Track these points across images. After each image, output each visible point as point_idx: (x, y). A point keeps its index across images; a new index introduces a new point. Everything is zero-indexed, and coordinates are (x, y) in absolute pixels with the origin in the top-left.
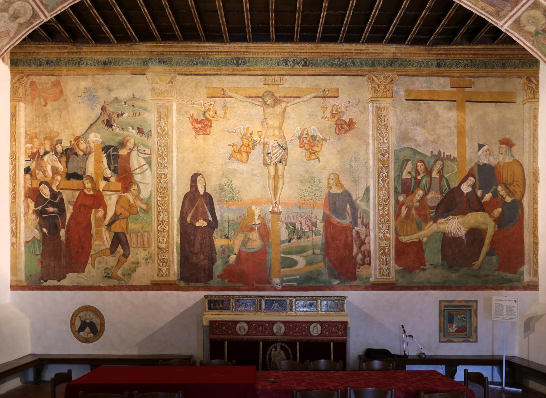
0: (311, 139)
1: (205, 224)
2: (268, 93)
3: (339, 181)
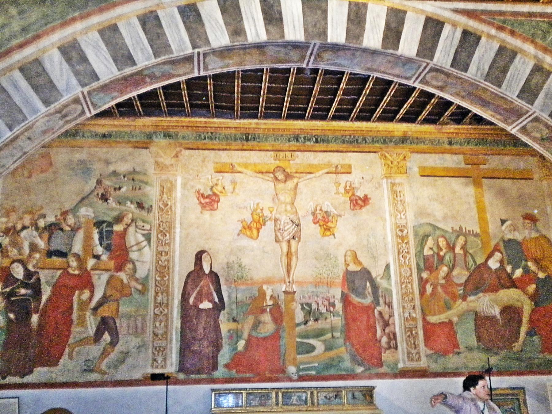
0: (325, 215)
1: (210, 305)
3: (356, 257)
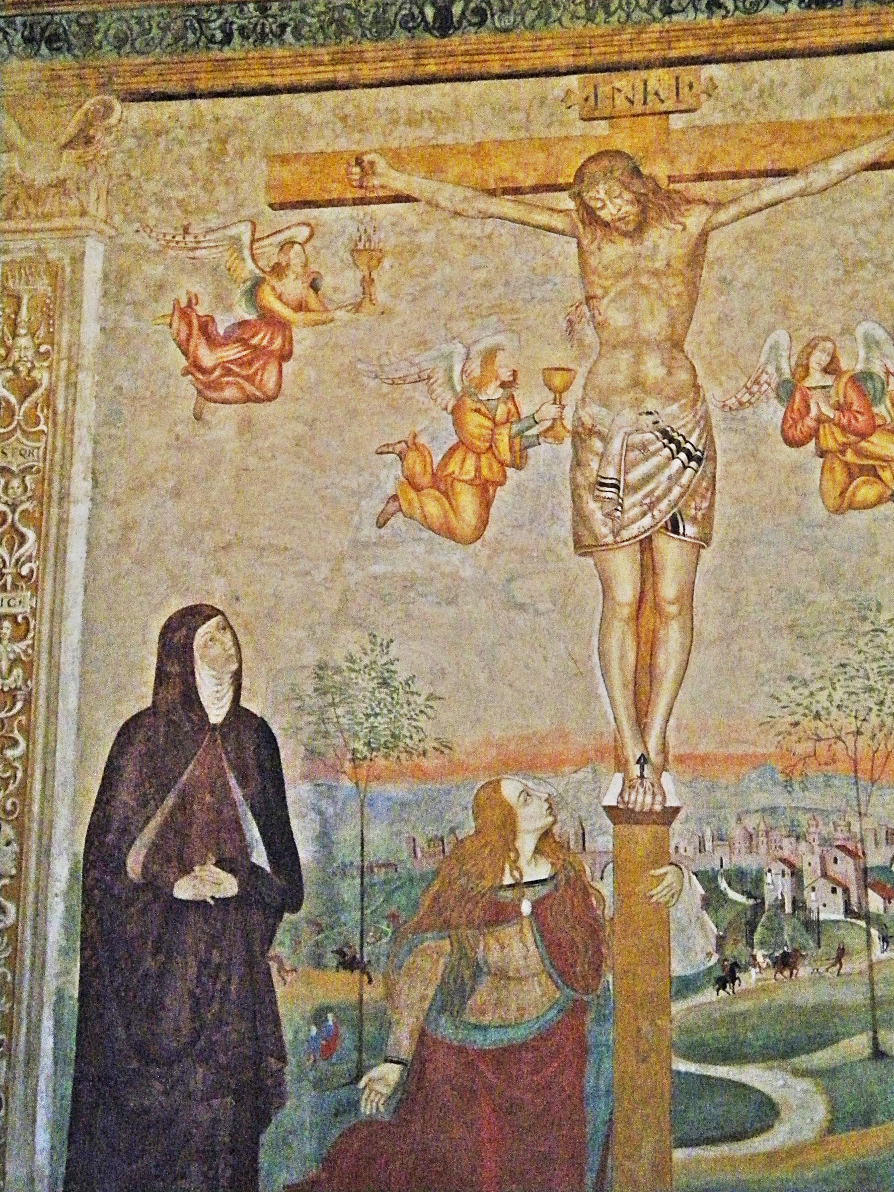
0: (853, 396)
1: (229, 886)
2: (605, 162)
